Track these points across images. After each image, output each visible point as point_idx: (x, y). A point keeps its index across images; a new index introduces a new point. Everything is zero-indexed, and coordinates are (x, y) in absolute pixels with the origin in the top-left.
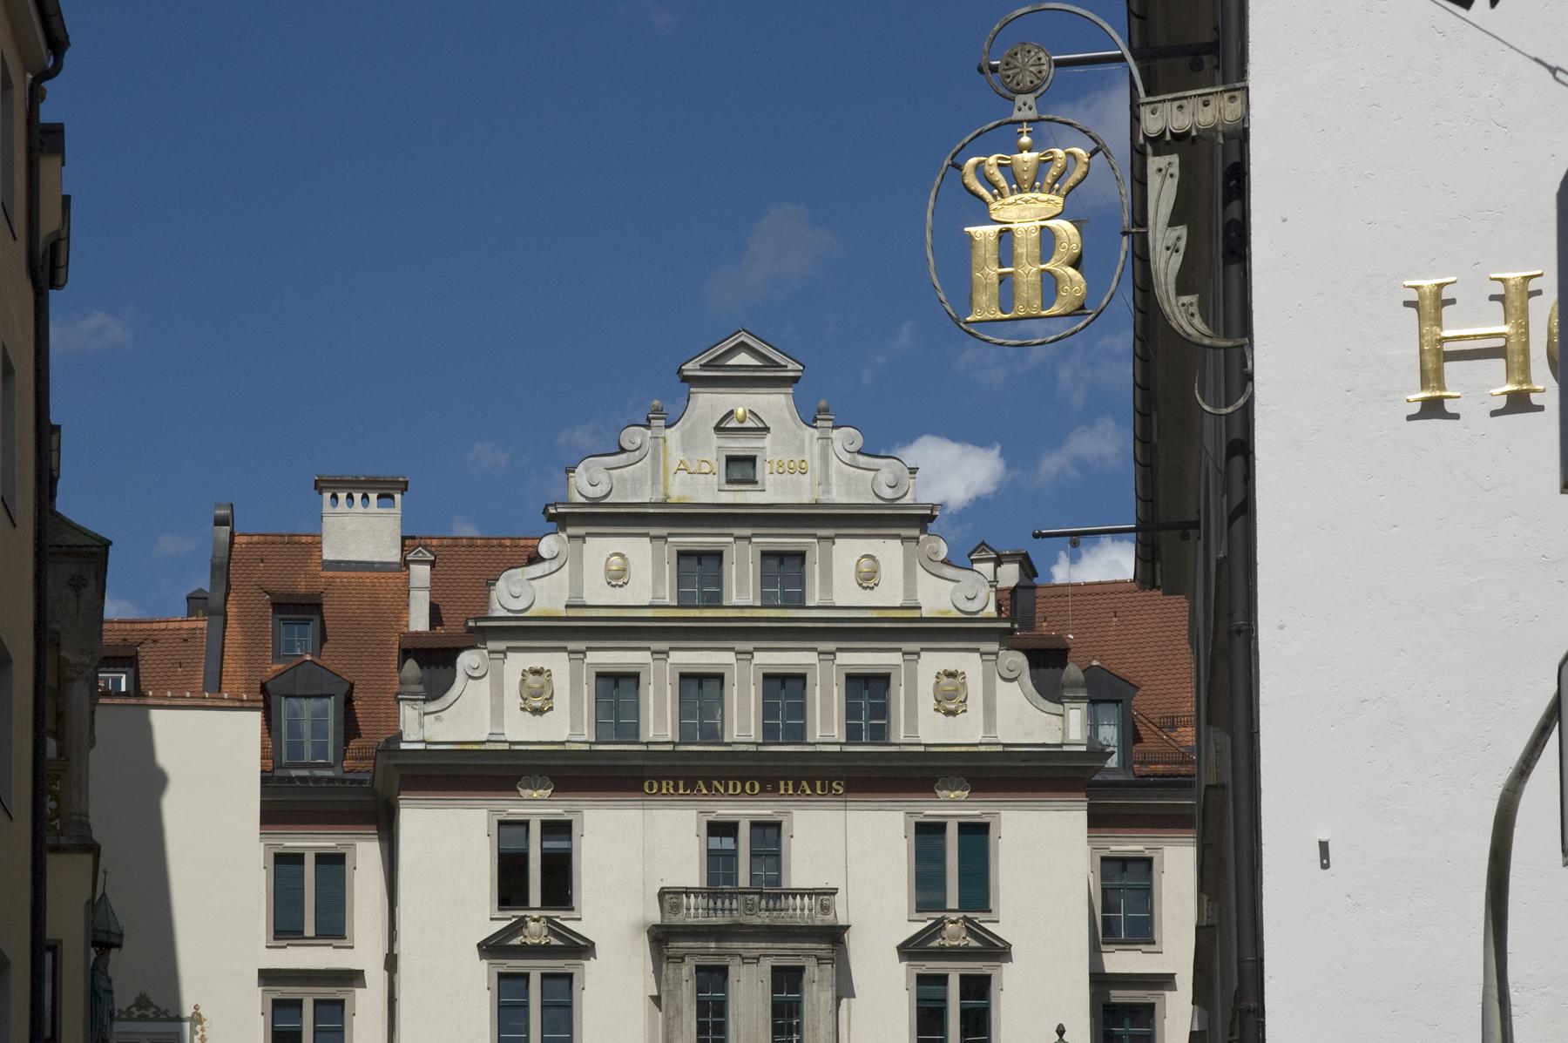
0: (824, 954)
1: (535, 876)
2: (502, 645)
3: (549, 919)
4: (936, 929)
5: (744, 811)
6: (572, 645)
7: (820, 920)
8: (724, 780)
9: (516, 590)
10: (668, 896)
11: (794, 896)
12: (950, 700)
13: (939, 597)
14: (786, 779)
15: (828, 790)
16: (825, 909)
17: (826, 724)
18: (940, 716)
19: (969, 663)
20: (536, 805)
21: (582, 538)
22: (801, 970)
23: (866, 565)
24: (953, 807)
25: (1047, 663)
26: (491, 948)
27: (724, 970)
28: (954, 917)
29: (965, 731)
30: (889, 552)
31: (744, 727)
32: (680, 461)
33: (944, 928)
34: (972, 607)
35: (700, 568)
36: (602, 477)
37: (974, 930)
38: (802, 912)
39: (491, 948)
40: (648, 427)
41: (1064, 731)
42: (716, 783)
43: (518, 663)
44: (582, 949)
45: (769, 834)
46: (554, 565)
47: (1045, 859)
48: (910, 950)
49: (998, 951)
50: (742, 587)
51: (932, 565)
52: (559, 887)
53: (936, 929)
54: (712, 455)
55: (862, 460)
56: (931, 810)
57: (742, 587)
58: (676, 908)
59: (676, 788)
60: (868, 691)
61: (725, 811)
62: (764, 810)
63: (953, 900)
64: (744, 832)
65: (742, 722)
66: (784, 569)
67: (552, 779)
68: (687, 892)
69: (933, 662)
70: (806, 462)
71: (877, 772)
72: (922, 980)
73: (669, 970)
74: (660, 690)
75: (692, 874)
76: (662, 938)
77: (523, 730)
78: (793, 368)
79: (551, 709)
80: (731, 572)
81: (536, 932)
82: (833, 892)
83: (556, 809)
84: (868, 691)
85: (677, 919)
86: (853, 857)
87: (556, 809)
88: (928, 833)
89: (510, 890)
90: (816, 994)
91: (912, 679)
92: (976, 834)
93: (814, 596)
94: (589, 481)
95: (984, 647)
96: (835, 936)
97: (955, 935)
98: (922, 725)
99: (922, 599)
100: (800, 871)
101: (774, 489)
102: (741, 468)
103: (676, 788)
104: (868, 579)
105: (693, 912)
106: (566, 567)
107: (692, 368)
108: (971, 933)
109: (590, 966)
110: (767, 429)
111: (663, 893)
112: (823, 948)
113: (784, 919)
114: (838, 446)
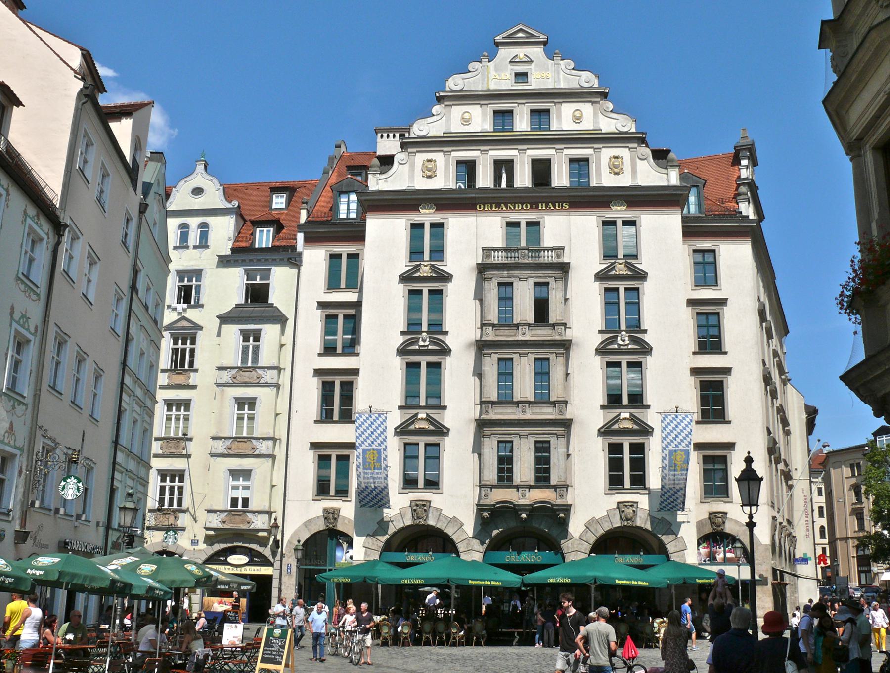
0: (558, 276)
1: (426, 246)
2: (415, 150)
3: (432, 265)
4: (612, 267)
5: (523, 216)
6: (445, 149)
7: (555, 260)
8: (514, 203)
9: (421, 128)
10: (487, 251)
11: (544, 250)
12: (616, 170)
13: (609, 124)
14: (542, 203)
17: (561, 178)
18: (612, 175)
19: (624, 153)
20: (427, 216)
21: (451, 106)
22: (548, 284)
25: (660, 156)
26: (405, 279)
27: (511, 284)
28: (621, 261)
29: (624, 181)
30: (587, 109)
31: (522, 181)
34: (625, 129)
35: (503, 116)
36: (460, 82)
37: (630, 266)
38: (548, 257)
39: (405, 279)
40: (480, 62)
43: (420, 158)
44: (446, 278)
45: (534, 225)
46: (439, 117)
47: (661, 237)
48: (600, 277)
49: (641, 276)
50: (522, 123)
51: (604, 112)
52: (438, 252)
53: (612, 267)
55: (574, 72)
57: (522, 123)
58: (489, 256)
59: (491, 207)
60: (580, 165)
61: (514, 217)
62: (532, 216)
64: (523, 225)
65: (523, 178)
66: (540, 116)
68: (494, 249)
69: (607, 153)
70: (549, 73)
74: (485, 166)
75: (498, 241)
76: (483, 269)
77: (422, 184)
78: (543, 38)
80: (517, 117)
81: (425, 271)
82: (563, 249)
83: (437, 217)
84: (580, 165)
85: (491, 260)
87: (437, 217)
89: (415, 253)
91: (599, 160)
93: (554, 126)
95: (631, 145)
96: (563, 268)
97: (621, 269)
98: (603, 177)
99: (602, 128)
100: (548, 241)
101: (535, 83)
102: (521, 76)
103: (491, 207)
105: (498, 258)
107: (499, 38)
108: (630, 269)
109: (450, 285)
112: (558, 274)
113: (542, 260)
114: (563, 67)
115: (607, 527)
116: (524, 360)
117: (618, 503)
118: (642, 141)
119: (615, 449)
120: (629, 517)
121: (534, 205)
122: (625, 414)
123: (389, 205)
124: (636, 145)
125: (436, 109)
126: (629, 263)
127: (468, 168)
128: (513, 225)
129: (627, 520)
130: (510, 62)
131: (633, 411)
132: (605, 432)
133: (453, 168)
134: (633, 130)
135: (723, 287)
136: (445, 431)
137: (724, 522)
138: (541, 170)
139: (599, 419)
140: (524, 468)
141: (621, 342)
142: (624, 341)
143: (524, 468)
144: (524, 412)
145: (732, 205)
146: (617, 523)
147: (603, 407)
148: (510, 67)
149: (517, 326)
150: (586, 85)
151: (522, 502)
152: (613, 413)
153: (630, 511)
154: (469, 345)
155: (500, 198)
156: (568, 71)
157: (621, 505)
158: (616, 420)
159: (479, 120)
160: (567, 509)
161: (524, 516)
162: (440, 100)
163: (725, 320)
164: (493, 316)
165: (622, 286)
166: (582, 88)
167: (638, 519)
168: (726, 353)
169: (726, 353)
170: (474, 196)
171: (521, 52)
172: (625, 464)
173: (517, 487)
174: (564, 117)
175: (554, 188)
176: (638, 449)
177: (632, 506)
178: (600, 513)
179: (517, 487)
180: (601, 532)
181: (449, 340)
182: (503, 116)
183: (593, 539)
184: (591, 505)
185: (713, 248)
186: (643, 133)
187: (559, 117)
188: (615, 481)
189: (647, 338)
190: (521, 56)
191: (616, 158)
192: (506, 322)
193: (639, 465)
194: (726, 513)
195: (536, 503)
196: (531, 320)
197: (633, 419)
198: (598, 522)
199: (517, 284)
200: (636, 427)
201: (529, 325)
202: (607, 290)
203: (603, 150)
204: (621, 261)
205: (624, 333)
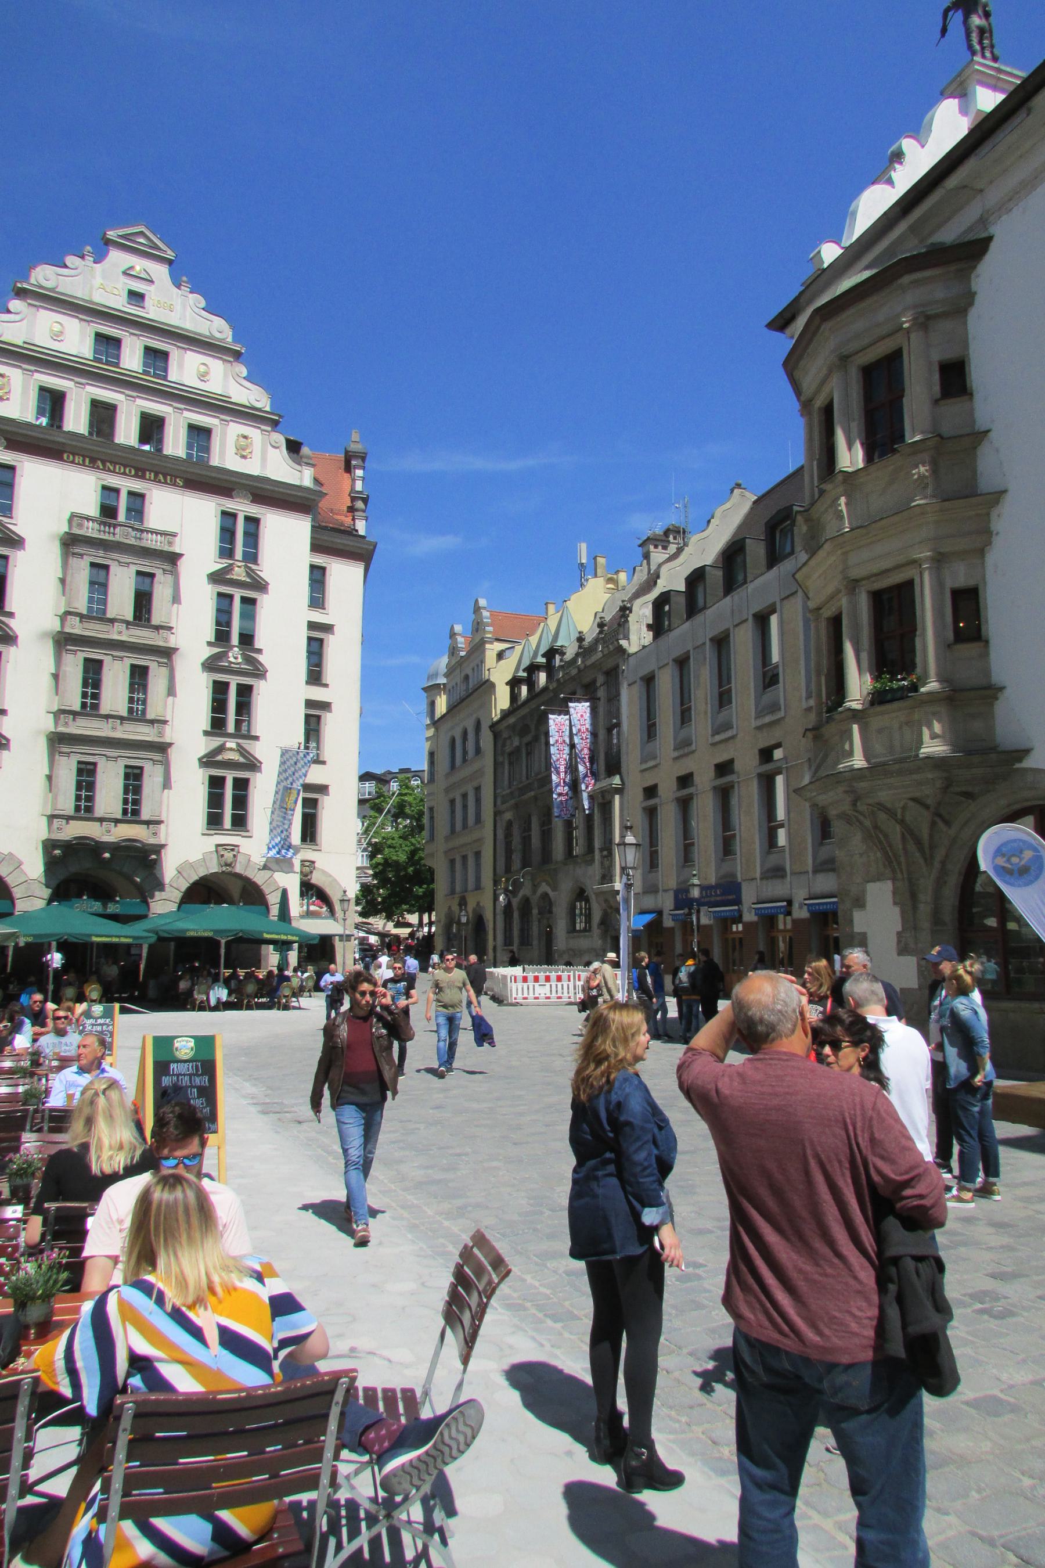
4: (229, 569)
7: (166, 548)
8: (115, 463)
10: (75, 518)
14: (151, 471)
15: (175, 485)
16: (170, 543)
17: (175, 444)
18: (238, 457)
19: (255, 434)
23: (203, 369)
24: (243, 507)
28: (240, 564)
29: (251, 467)
30: (217, 366)
31: (127, 437)
32: (101, 279)
33: (232, 569)
34: (258, 405)
35: (108, 344)
36: (53, 277)
37: (250, 572)
41: (301, 479)
42: (108, 464)
45: (137, 499)
48: (216, 578)
49: (260, 586)
50: (132, 358)
53: (229, 569)
54: (119, 286)
55: (204, 313)
56: (230, 505)
57: (132, 358)
58: (80, 526)
59: (84, 461)
60: (199, 434)
61: (113, 481)
62: (137, 486)
63: (239, 554)
65: (127, 432)
66: (156, 357)
67: (6, 439)
68: (88, 519)
70: (176, 305)
71: (201, 478)
72: (220, 595)
73: (73, 561)
75: (92, 509)
76: (71, 543)
78: (170, 254)
79: (8, 399)
82: (174, 535)
84: (199, 434)
86: (185, 519)
88: (229, 516)
90: (161, 592)
91: (224, 434)
92: (253, 522)
93: (173, 375)
94: (44, 276)
96: (173, 559)
97: (239, 573)
99: (231, 395)
103: (84, 461)
104: (203, 377)
105: (91, 530)
106: (25, 322)
107: (111, 234)
108: (248, 575)
110: (152, 282)
111: (73, 516)
113: (144, 543)
114: (191, 302)
115: (202, 872)
116: (118, 664)
117: (218, 846)
118: (275, 424)
119: (216, 784)
120: (229, 861)
121: (140, 473)
122: (231, 744)
123: (292, 503)
124: (269, 429)
125: (15, 304)
126: (250, 568)
127: (53, 402)
128: (109, 491)
129: (226, 865)
130: (125, 273)
131: (240, 741)
132: (208, 761)
133: (33, 395)
134: (268, 409)
135: (330, 612)
136: (4, 742)
137: (311, 872)
138: (152, 428)
139: (203, 746)
140: (109, 794)
141: (232, 659)
142: (236, 658)
143: (109, 794)
144: (114, 728)
145: (347, 520)
146: (214, 868)
147: (206, 733)
148: (124, 279)
149: (112, 621)
150: (218, 335)
151: (106, 839)
152: (216, 742)
153: (231, 854)
154: (45, 635)
155: (95, 448)
156: (197, 310)
157: (220, 848)
158: (221, 749)
159: (76, 339)
160: (158, 849)
161: (107, 855)
162: (21, 293)
163: (330, 649)
164: (82, 605)
165: (238, 594)
166: (212, 337)
167: (238, 865)
168: (326, 686)
169: (326, 686)
170: (64, 441)
171: (140, 264)
172: (227, 800)
173: (101, 820)
174: (187, 369)
175: (166, 456)
176: (242, 786)
177: (233, 850)
178: (195, 856)
179: (101, 820)
180: (195, 878)
181: (16, 625)
182: (108, 344)
183: (184, 886)
184: (186, 845)
185: (324, 565)
186: (280, 416)
187: (181, 366)
188: (214, 821)
189: (261, 658)
190: (138, 268)
191: (245, 437)
192: (98, 614)
193: (241, 802)
194: (313, 862)
195: (124, 841)
196: (130, 617)
197: (241, 750)
198: (192, 865)
199: (114, 569)
200: (242, 760)
201: (128, 623)
202: (220, 595)
203: (231, 424)
204: (240, 564)
205: (236, 649)
